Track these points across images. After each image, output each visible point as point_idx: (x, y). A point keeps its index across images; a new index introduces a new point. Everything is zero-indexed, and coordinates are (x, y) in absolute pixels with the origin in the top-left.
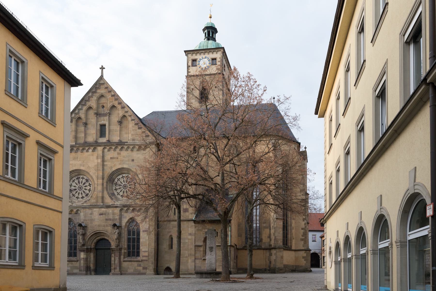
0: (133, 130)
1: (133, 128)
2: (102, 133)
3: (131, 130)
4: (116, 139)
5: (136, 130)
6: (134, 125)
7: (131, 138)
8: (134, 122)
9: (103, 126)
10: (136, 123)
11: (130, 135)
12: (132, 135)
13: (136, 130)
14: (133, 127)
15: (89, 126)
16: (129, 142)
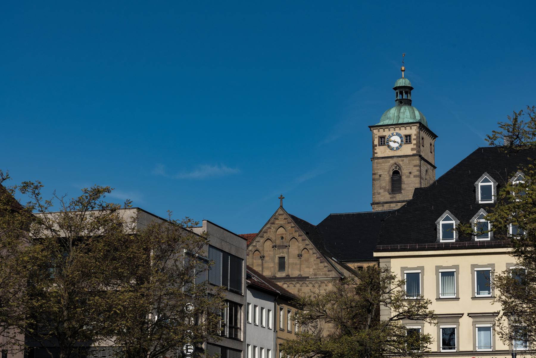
0: (315, 264)
1: (315, 262)
2: (282, 265)
3: (313, 264)
4: (295, 273)
5: (318, 264)
6: (315, 258)
7: (312, 273)
8: (315, 255)
9: (282, 259)
10: (318, 257)
11: (311, 270)
12: (314, 269)
13: (318, 264)
14: (315, 261)
15: (266, 259)
16: (310, 277)
